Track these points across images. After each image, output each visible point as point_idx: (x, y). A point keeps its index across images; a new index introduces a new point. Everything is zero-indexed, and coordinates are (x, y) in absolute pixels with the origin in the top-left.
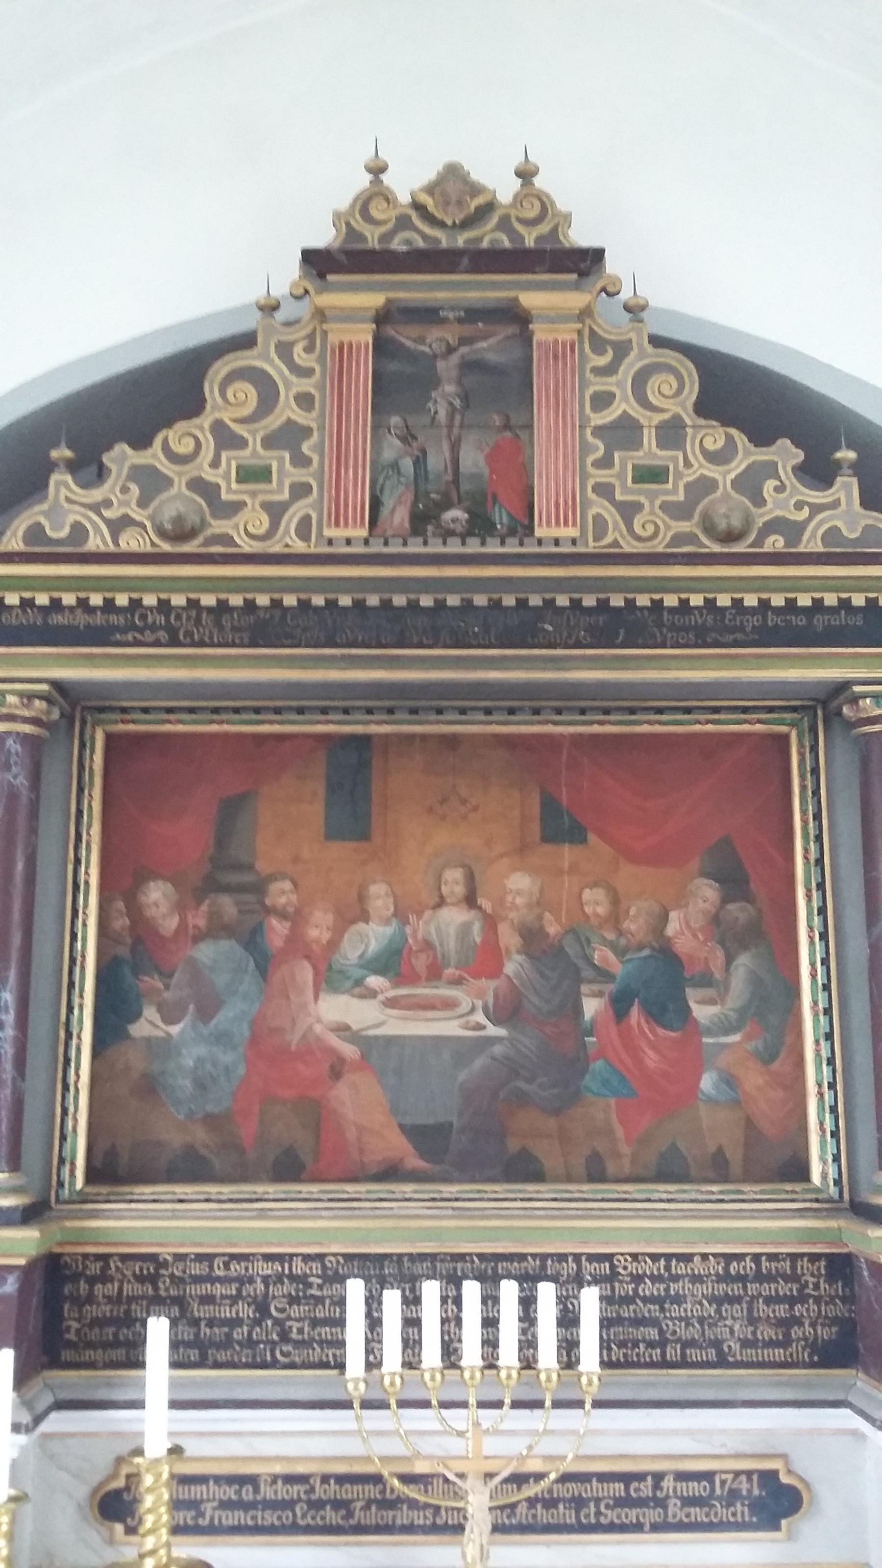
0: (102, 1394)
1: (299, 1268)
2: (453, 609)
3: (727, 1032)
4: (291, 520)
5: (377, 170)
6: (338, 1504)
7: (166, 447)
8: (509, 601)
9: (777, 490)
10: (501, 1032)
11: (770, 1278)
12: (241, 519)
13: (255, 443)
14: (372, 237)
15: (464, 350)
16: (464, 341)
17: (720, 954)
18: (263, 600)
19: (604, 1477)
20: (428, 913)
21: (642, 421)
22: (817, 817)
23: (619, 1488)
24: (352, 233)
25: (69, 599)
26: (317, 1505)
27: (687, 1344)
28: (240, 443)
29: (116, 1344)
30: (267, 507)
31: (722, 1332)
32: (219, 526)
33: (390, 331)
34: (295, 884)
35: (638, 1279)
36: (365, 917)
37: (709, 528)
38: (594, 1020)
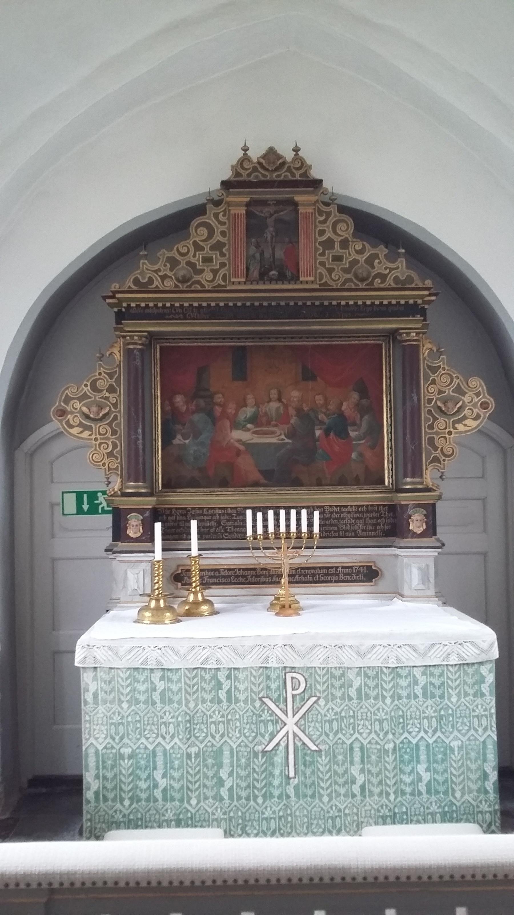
0: (172, 547)
1: (229, 511)
2: (274, 306)
3: (360, 440)
5: (245, 149)
6: (243, 576)
8: (292, 303)
10: (290, 441)
11: (371, 512)
12: (204, 275)
13: (207, 249)
14: (244, 178)
15: (276, 215)
16: (276, 212)
17: (359, 415)
18: (213, 304)
19: (320, 568)
20: (266, 404)
21: (335, 240)
22: (390, 371)
23: (325, 571)
24: (237, 174)
25: (151, 304)
26: (238, 577)
27: (347, 531)
28: (203, 249)
29: (175, 534)
30: (213, 271)
31: (356, 528)
32: (197, 278)
33: (251, 209)
35: (331, 513)
36: (246, 405)
37: (356, 276)
38: (319, 437)
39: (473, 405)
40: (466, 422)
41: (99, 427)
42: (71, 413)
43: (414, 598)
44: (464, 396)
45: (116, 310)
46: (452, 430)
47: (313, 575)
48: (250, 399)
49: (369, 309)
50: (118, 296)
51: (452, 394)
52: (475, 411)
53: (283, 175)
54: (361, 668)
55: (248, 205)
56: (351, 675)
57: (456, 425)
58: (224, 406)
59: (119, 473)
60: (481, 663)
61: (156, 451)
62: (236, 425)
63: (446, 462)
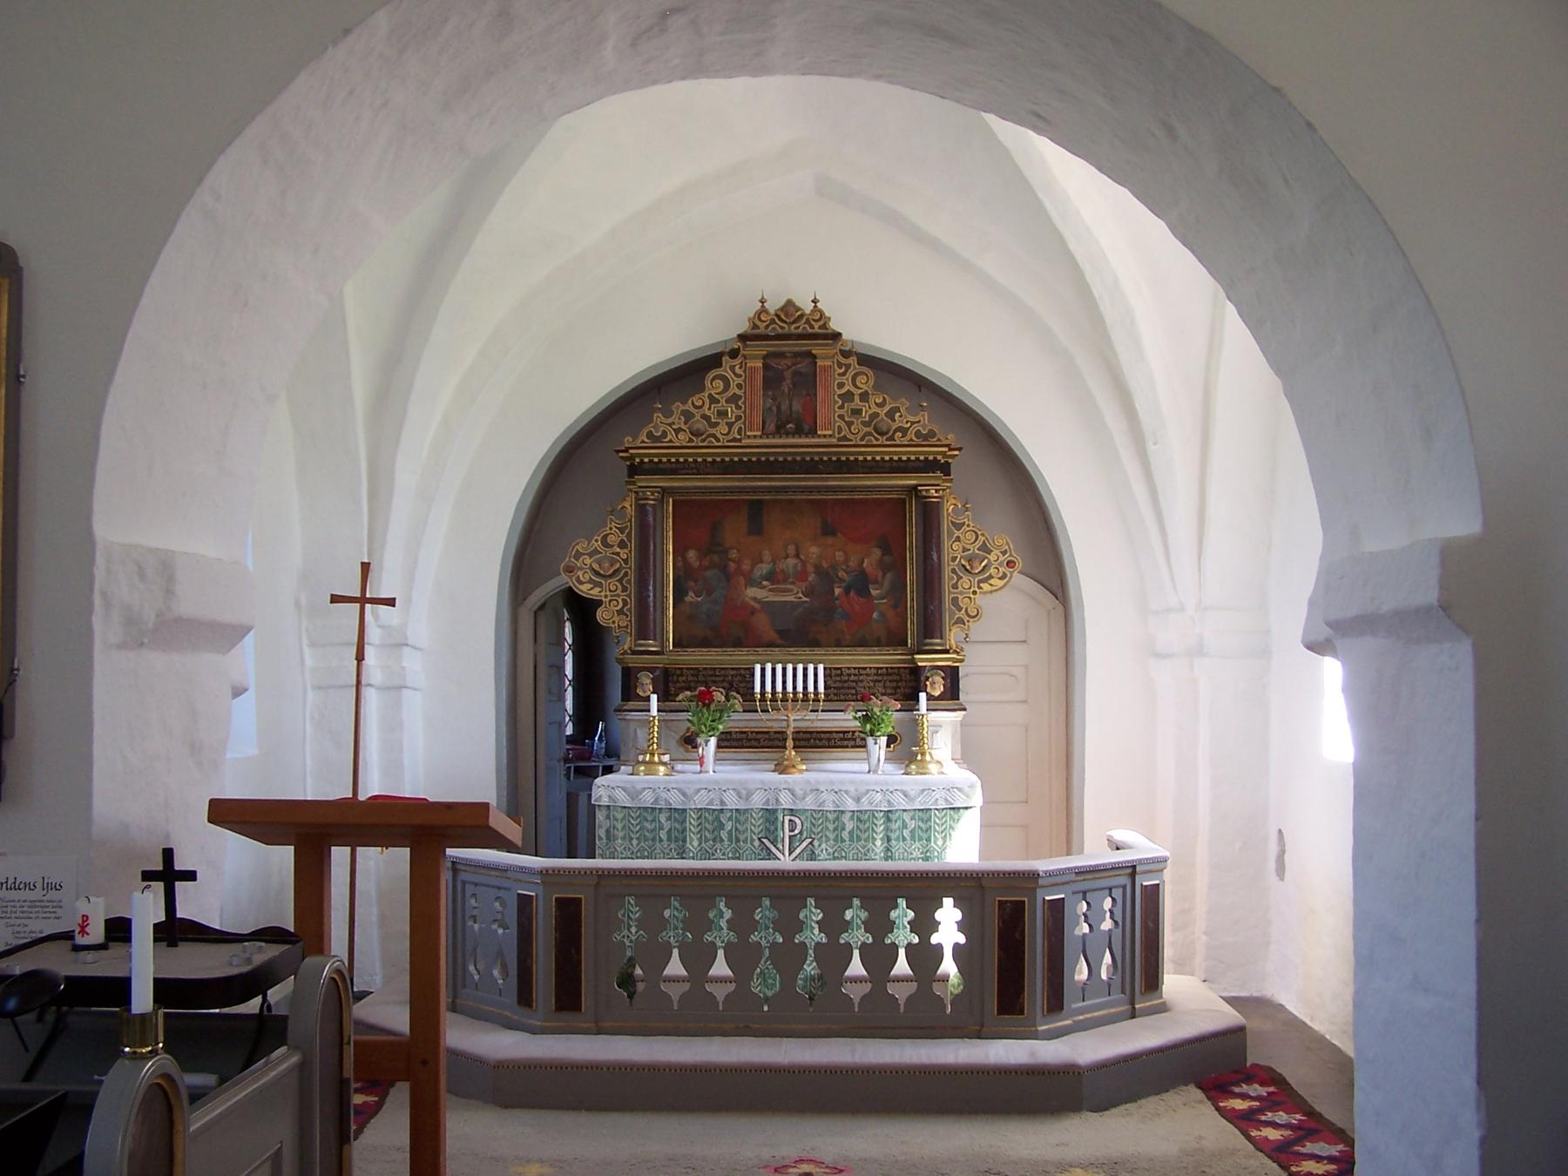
1: (743, 672)
4: (735, 429)
5: (762, 301)
6: (755, 740)
7: (693, 404)
8: (808, 459)
9: (901, 416)
11: (891, 675)
15: (794, 367)
17: (881, 573)
18: (727, 459)
19: (836, 732)
23: (841, 735)
24: (755, 327)
25: (664, 460)
26: (749, 740)
30: (727, 423)
32: (712, 431)
34: (738, 550)
35: (849, 675)
36: (762, 562)
37: (876, 429)
38: (839, 595)
39: (998, 564)
40: (992, 581)
41: (610, 583)
42: (581, 569)
44: (990, 554)
45: (628, 463)
46: (976, 589)
47: (829, 740)
48: (767, 555)
49: (888, 465)
50: (631, 451)
51: (977, 551)
53: (802, 327)
54: (853, 811)
55: (764, 358)
56: (846, 818)
57: (981, 585)
58: (739, 562)
59: (629, 631)
61: (667, 609)
62: (751, 582)
63: (970, 623)
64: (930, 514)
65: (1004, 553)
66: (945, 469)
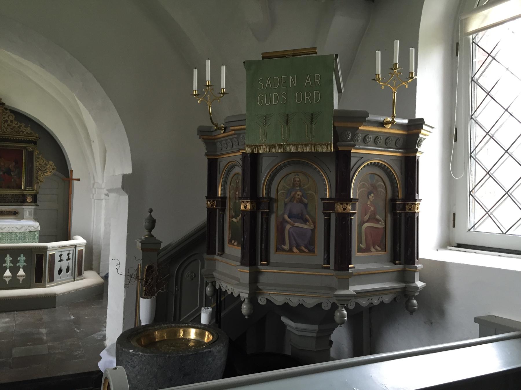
38: (2, 174)
40: (48, 173)
43: (27, 219)
52: (50, 170)
54: (1, 233)
60: (35, 231)
64: (30, 155)
65: (51, 166)
66: (35, 143)
